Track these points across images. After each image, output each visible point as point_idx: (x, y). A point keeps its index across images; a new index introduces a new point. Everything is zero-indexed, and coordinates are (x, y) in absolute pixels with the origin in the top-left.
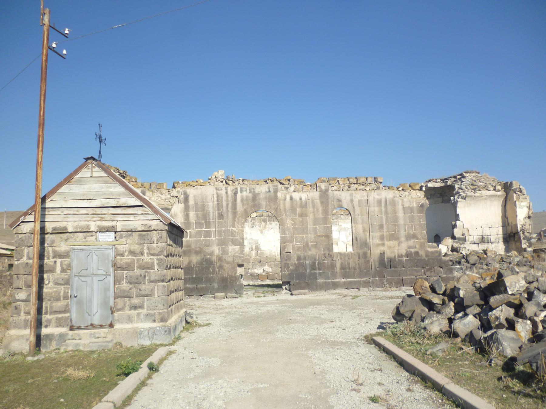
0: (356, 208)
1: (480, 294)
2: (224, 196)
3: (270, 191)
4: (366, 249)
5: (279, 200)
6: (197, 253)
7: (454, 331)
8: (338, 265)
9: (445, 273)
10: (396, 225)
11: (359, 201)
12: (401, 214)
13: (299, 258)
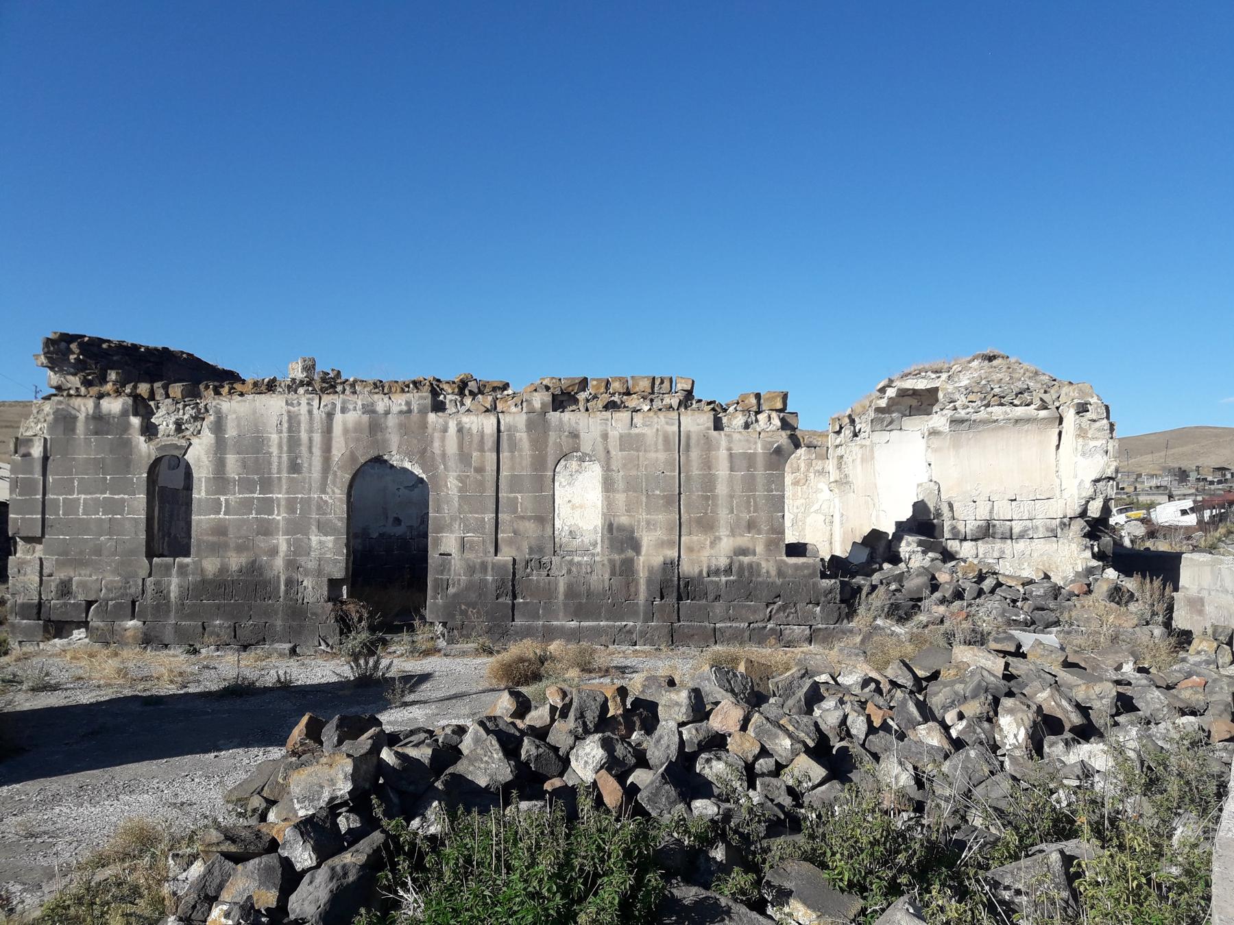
0: (613, 453)
1: (348, 555)
2: (304, 418)
3: (409, 411)
4: (630, 553)
5: (430, 430)
6: (240, 549)
7: (213, 534)
8: (562, 588)
9: (825, 620)
10: (707, 498)
11: (621, 436)
12: (722, 471)
13: (471, 569)
